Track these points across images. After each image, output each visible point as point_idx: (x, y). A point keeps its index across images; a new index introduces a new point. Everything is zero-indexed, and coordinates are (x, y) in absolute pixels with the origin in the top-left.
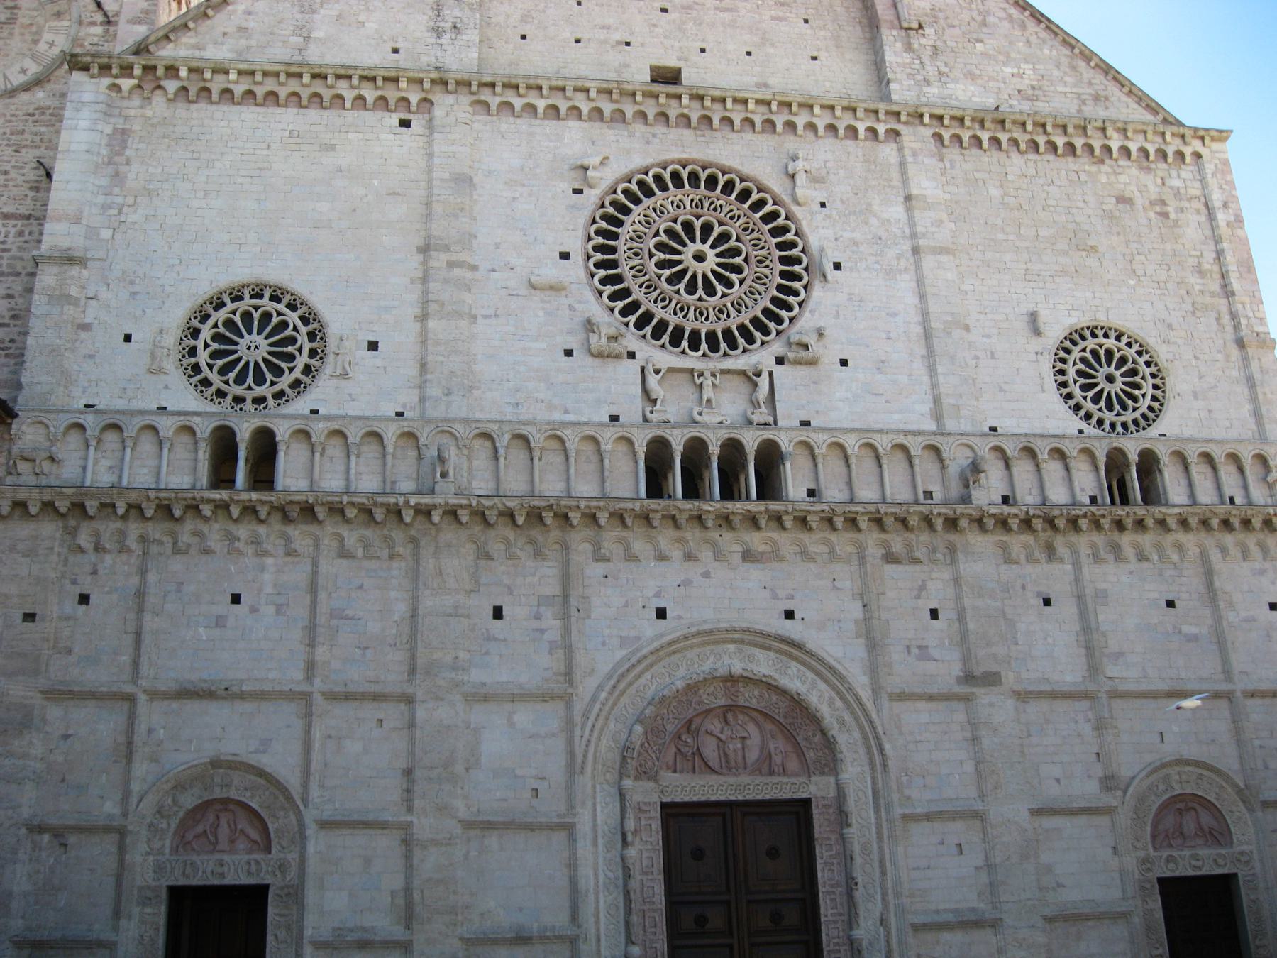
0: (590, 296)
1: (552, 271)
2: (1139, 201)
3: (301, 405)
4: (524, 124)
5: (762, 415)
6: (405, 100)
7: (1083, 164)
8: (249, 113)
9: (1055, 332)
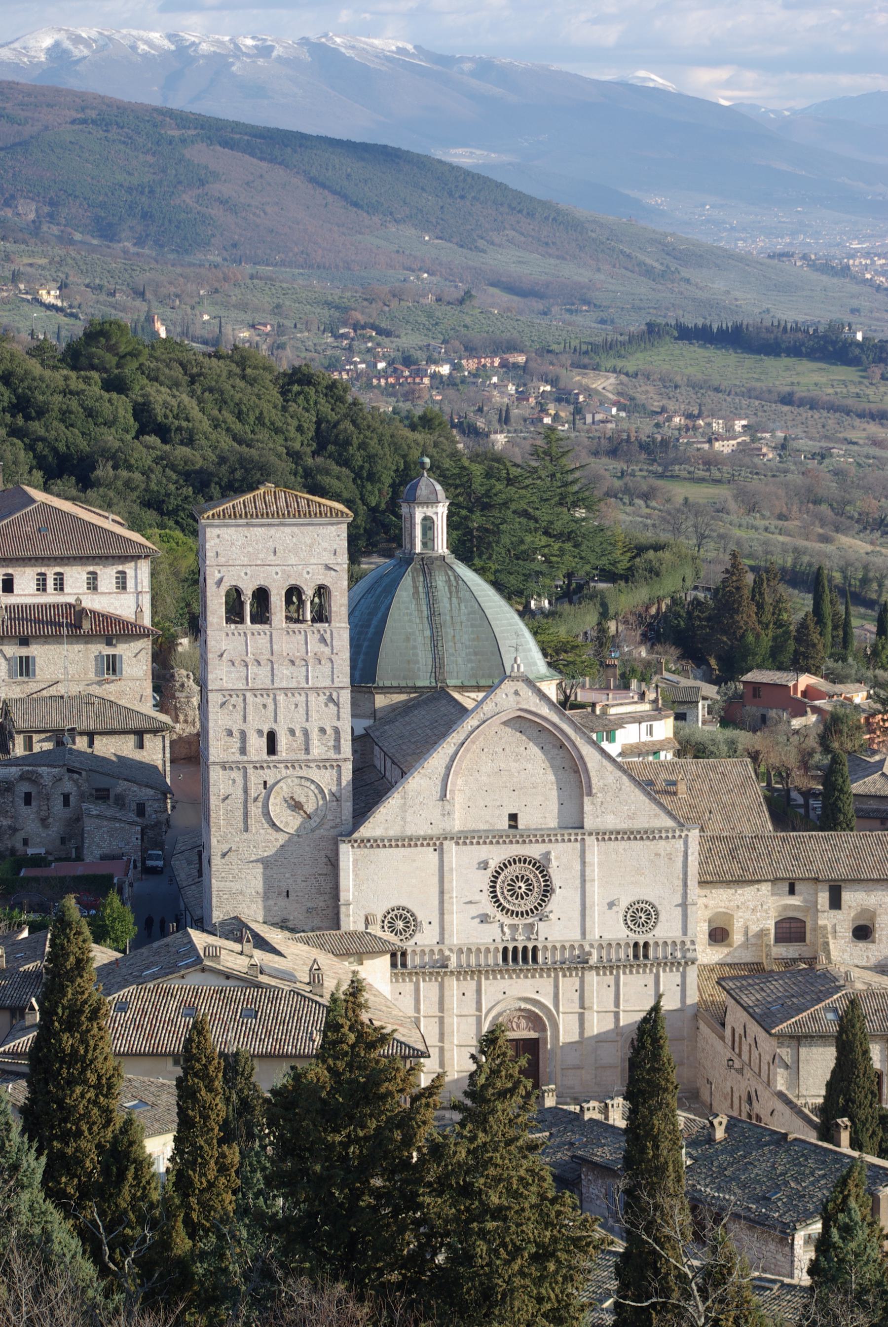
0: (488, 903)
1: (477, 897)
2: (663, 853)
3: (412, 942)
4: (470, 847)
5: (534, 936)
6: (435, 844)
7: (648, 843)
8: (391, 850)
9: (624, 904)
